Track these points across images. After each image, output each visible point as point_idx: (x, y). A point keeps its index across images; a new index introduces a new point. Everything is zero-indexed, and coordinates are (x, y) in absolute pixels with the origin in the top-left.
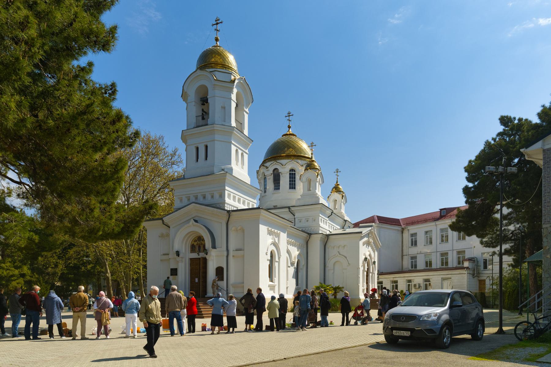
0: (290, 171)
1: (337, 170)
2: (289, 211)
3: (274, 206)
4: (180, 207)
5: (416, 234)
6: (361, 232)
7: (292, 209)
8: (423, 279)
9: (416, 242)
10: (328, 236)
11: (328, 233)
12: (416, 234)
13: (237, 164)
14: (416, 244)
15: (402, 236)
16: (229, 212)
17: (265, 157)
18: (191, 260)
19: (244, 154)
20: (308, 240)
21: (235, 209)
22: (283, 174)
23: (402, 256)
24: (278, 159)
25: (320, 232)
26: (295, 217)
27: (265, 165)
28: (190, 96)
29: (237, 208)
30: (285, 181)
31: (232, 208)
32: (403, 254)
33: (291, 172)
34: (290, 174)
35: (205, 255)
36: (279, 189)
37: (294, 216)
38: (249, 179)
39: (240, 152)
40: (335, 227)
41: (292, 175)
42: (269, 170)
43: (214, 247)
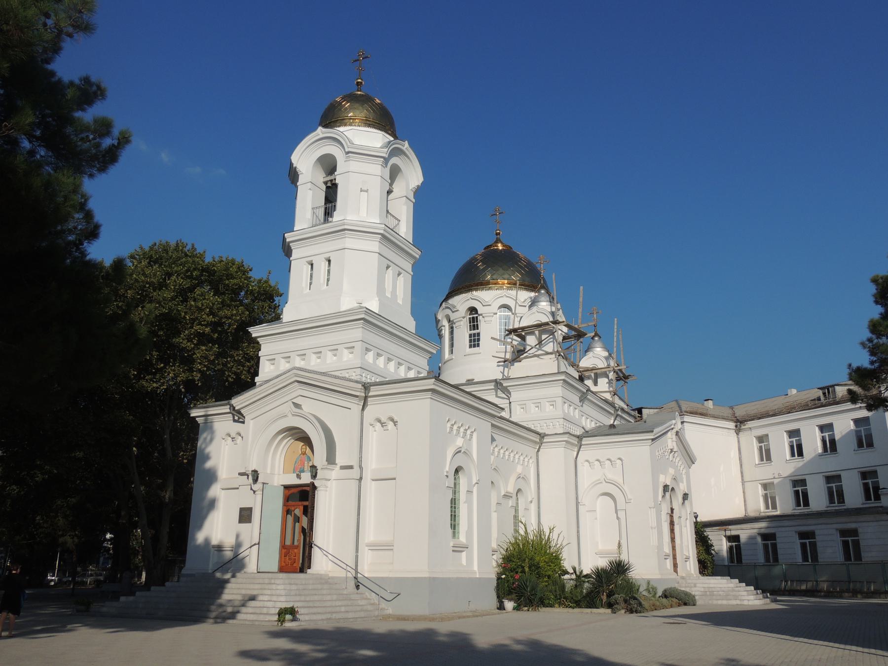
3: (469, 380)
4: (267, 379)
5: (767, 435)
9: (768, 452)
12: (767, 435)
14: (769, 458)
17: (451, 288)
18: (287, 487)
22: (486, 316)
23: (743, 482)
24: (476, 290)
27: (451, 301)
28: (302, 173)
32: (746, 479)
33: (502, 314)
36: (478, 345)
42: (458, 311)
43: (331, 459)
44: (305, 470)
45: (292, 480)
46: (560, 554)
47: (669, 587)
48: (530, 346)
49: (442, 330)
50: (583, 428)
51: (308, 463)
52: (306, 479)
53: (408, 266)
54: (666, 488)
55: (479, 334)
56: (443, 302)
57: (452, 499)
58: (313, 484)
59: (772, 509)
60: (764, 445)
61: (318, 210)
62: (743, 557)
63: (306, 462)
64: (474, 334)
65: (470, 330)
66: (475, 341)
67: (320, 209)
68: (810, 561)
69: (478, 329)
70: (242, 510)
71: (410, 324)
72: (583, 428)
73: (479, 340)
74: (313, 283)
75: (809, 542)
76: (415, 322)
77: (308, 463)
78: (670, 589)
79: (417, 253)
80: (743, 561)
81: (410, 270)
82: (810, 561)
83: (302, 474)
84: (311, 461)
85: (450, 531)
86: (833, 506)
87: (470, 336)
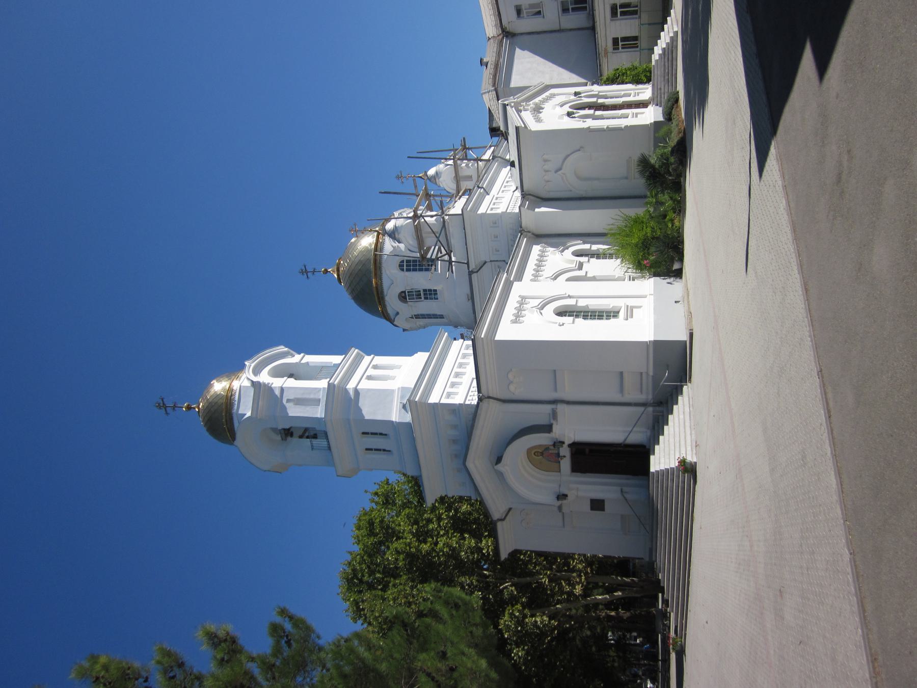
0: (403, 270)
1: (398, 177)
2: (477, 272)
6: (517, 128)
7: (474, 267)
8: (611, 20)
10: (524, 195)
11: (518, 194)
13: (393, 378)
15: (522, 34)
16: (480, 399)
17: (381, 317)
19: (374, 363)
20: (533, 234)
21: (475, 383)
25: (517, 210)
26: (488, 260)
29: (473, 379)
30: (419, 280)
31: (472, 389)
32: (558, 28)
34: (408, 270)
35: (565, 446)
36: (435, 290)
37: (485, 263)
38: (420, 353)
39: (371, 372)
40: (507, 179)
41: (410, 266)
44: (557, 452)
45: (566, 464)
46: (631, 217)
47: (662, 115)
48: (437, 242)
49: (419, 325)
50: (514, 192)
51: (551, 450)
52: (565, 451)
53: (367, 359)
54: (569, 114)
55: (425, 290)
56: (393, 324)
57: (583, 318)
58: (570, 446)
59: (587, 4)
60: (525, 9)
61: (314, 445)
62: (634, 34)
63: (550, 452)
64: (424, 294)
65: (421, 298)
66: (430, 294)
67: (314, 442)
68: (637, 8)
69: (420, 291)
70: (592, 508)
71: (421, 357)
72: (514, 192)
73: (430, 290)
74: (384, 448)
75: (621, 42)
76: (419, 353)
77: (551, 450)
78: (663, 115)
79: (354, 352)
80: (637, 35)
81: (370, 357)
82: (637, 8)
83: (561, 455)
84: (549, 448)
85: (613, 320)
86: (589, 8)
87: (426, 298)
